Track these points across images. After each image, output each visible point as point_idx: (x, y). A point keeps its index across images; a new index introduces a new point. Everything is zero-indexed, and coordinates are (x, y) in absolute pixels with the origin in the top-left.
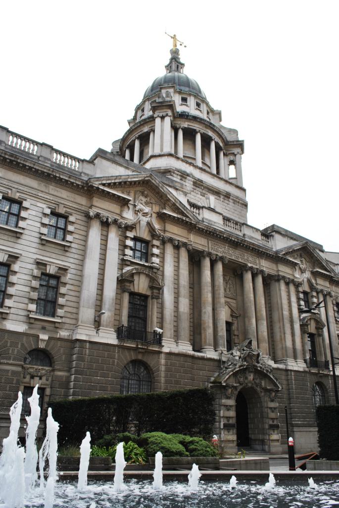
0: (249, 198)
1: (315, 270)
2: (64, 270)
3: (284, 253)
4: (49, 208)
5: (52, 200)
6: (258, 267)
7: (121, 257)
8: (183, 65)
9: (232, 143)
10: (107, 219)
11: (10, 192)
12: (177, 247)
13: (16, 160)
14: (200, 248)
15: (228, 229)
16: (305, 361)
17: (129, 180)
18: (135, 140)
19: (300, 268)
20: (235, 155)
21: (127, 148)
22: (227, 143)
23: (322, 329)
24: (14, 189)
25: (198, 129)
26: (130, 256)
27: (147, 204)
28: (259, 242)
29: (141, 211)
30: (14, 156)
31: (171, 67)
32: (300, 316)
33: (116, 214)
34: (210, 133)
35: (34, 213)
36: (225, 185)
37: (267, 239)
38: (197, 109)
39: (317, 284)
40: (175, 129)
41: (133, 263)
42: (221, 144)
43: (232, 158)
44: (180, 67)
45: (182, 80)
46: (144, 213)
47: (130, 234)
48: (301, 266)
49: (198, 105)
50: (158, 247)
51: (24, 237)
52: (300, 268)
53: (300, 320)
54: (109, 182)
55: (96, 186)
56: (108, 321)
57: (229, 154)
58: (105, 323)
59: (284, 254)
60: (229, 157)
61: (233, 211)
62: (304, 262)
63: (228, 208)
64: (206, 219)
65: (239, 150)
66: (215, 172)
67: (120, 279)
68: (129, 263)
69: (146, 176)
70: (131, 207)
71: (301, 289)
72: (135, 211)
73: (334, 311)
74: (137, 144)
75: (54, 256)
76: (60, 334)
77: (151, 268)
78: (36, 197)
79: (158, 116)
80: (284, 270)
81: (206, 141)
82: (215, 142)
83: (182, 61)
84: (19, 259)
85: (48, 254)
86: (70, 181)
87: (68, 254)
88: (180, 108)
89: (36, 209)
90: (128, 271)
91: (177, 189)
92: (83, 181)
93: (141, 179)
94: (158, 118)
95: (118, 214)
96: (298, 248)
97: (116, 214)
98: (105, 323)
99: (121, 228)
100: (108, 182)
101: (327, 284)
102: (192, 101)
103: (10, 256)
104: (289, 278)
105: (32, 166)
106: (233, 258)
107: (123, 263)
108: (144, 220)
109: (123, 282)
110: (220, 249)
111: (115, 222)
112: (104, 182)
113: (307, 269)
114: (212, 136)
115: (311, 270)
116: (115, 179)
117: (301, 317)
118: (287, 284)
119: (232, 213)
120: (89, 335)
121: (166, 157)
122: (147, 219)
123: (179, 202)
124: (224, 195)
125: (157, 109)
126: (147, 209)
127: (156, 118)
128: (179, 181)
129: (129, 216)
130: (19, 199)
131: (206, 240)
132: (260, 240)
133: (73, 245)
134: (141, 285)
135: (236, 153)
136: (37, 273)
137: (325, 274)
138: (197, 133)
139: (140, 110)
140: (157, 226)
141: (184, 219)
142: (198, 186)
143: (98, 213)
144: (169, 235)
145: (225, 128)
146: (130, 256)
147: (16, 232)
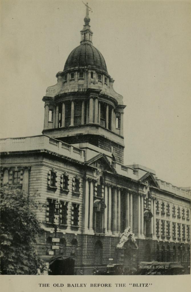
0: (125, 143)
8: (92, 33)
16: (144, 235)
27: (101, 167)
34: (112, 104)
38: (105, 84)
43: (118, 115)
49: (106, 79)
60: (116, 114)
62: (148, 182)
78: (72, 173)
79: (92, 97)
81: (111, 108)
82: (114, 109)
83: (92, 29)
102: (103, 77)
107: (95, 198)
109: (95, 208)
126: (100, 170)
135: (121, 113)
137: (155, 189)
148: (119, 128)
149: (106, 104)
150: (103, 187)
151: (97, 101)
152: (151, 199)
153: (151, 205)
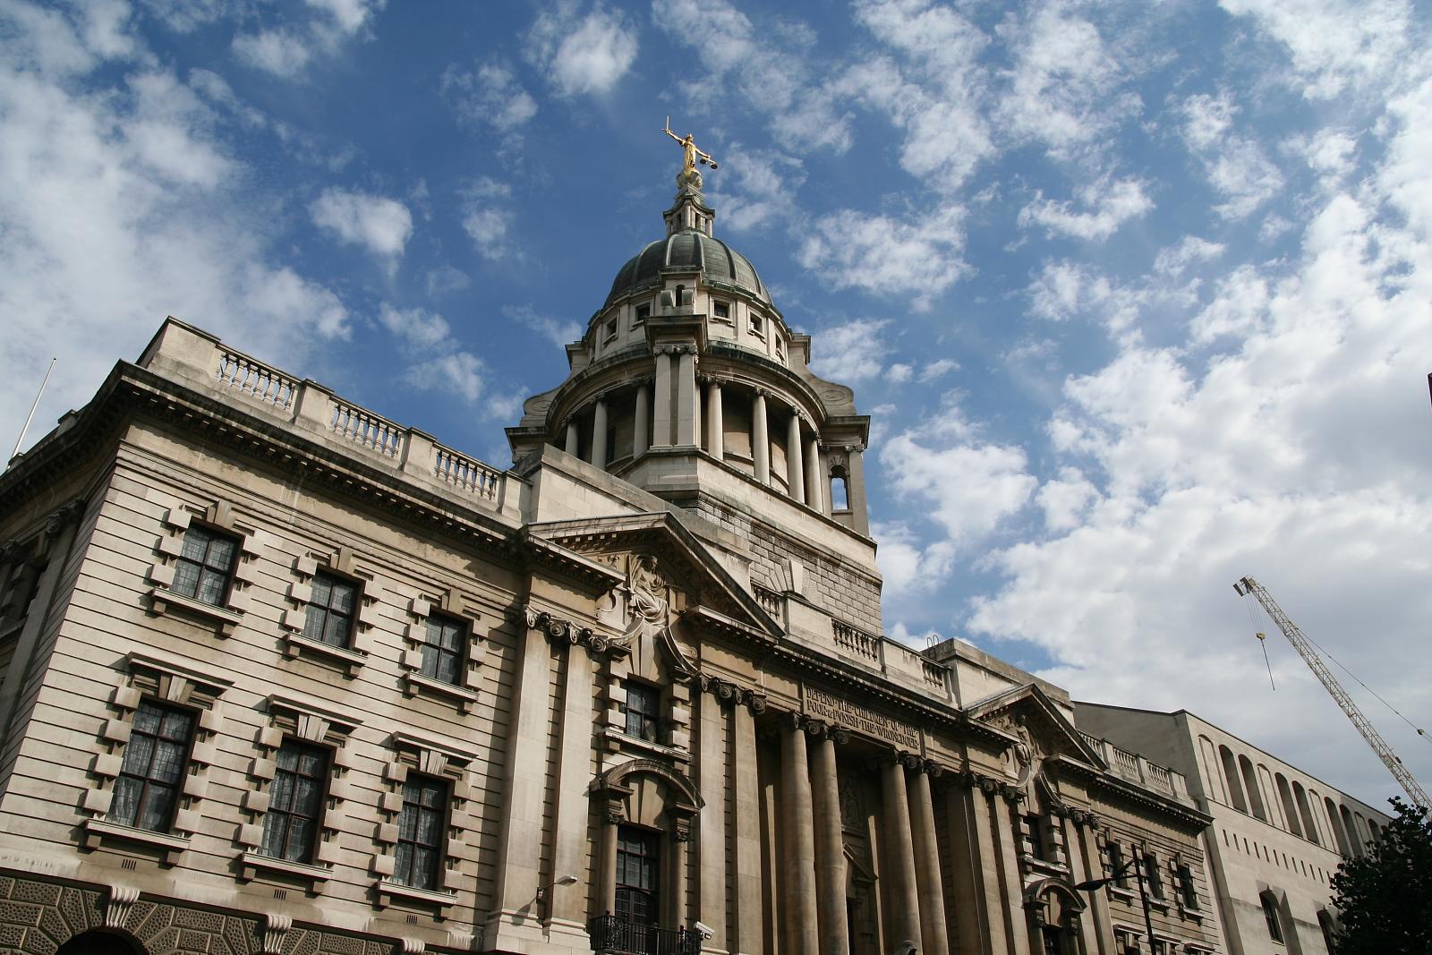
1: (1054, 757)
2: (459, 761)
3: (980, 714)
4: (427, 598)
5: (434, 579)
6: (918, 752)
7: (599, 730)
9: (840, 423)
10: (567, 631)
11: (335, 556)
12: (728, 706)
13: (353, 474)
14: (783, 704)
15: (846, 652)
17: (618, 529)
18: (595, 405)
19: (1018, 755)
20: (847, 454)
21: (571, 422)
22: (826, 424)
23: (1077, 915)
24: (344, 549)
25: (759, 387)
26: (620, 728)
28: (919, 685)
29: (643, 608)
30: (351, 464)
31: (680, 215)
32: (1022, 881)
33: (587, 616)
34: (790, 399)
35: (390, 612)
36: (827, 532)
37: (936, 678)
39: (1059, 794)
40: (705, 389)
41: (627, 748)
42: (814, 426)
43: (838, 460)
44: (702, 220)
45: (714, 256)
46: (650, 614)
47: (620, 669)
48: (1020, 747)
50: (684, 702)
51: (364, 673)
52: (1018, 755)
53: (1024, 891)
54: (569, 534)
55: (543, 545)
56: (570, 901)
57: (831, 449)
58: (562, 908)
59: (981, 718)
60: (830, 458)
61: (847, 600)
63: (834, 593)
64: (796, 628)
65: (858, 442)
66: (801, 500)
67: (595, 789)
68: (616, 746)
69: (657, 517)
70: (619, 598)
71: (1022, 809)
72: (630, 607)
73: (1103, 865)
74: (600, 415)
75: (437, 725)
76: (452, 936)
77: (669, 760)
79: (664, 352)
80: (980, 761)
82: (800, 419)
84: (352, 734)
85: (423, 721)
86: (477, 531)
87: (468, 720)
88: (715, 332)
89: (395, 600)
90: (617, 767)
91: (725, 550)
92: (510, 532)
93: (644, 526)
94: (663, 356)
95: (590, 617)
96: (1013, 701)
97: (587, 616)
98: (562, 908)
99: (596, 653)
100: (568, 534)
101: (1083, 795)
103: (334, 726)
104: (994, 780)
105: (391, 490)
106: (860, 730)
107: (602, 745)
108: (650, 631)
109: (601, 796)
110: (828, 707)
111: (584, 636)
112: (560, 534)
113: (1036, 756)
114: (792, 404)
115: (1043, 757)
116: (586, 527)
117: (1027, 885)
118: (990, 798)
119: (843, 606)
120: (527, 940)
121: (686, 459)
122: (658, 629)
123: (733, 585)
124: (825, 560)
125: (659, 334)
126: (657, 604)
127: (657, 355)
128: (717, 521)
129: (612, 617)
130: (464, 615)
131: (795, 687)
132: (920, 681)
133: (482, 697)
134: (647, 806)
136: (398, 770)
138: (757, 396)
139: (605, 326)
140: (683, 648)
141: (747, 630)
142: (763, 534)
143: (545, 613)
144: (710, 672)
145: (821, 382)
146: (620, 728)
147: (219, 622)
148: (849, 511)
149: (752, 395)
150: (680, 691)
151: (689, 365)
152: (1062, 817)
153: (1065, 849)
